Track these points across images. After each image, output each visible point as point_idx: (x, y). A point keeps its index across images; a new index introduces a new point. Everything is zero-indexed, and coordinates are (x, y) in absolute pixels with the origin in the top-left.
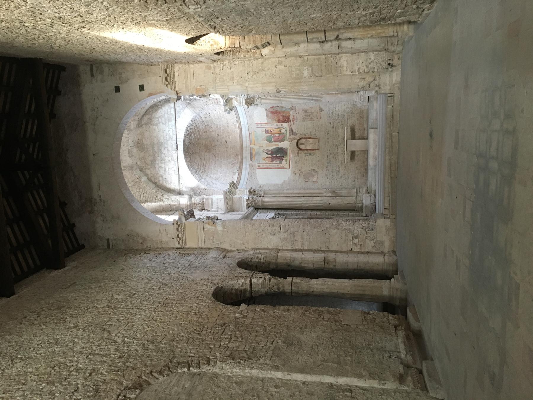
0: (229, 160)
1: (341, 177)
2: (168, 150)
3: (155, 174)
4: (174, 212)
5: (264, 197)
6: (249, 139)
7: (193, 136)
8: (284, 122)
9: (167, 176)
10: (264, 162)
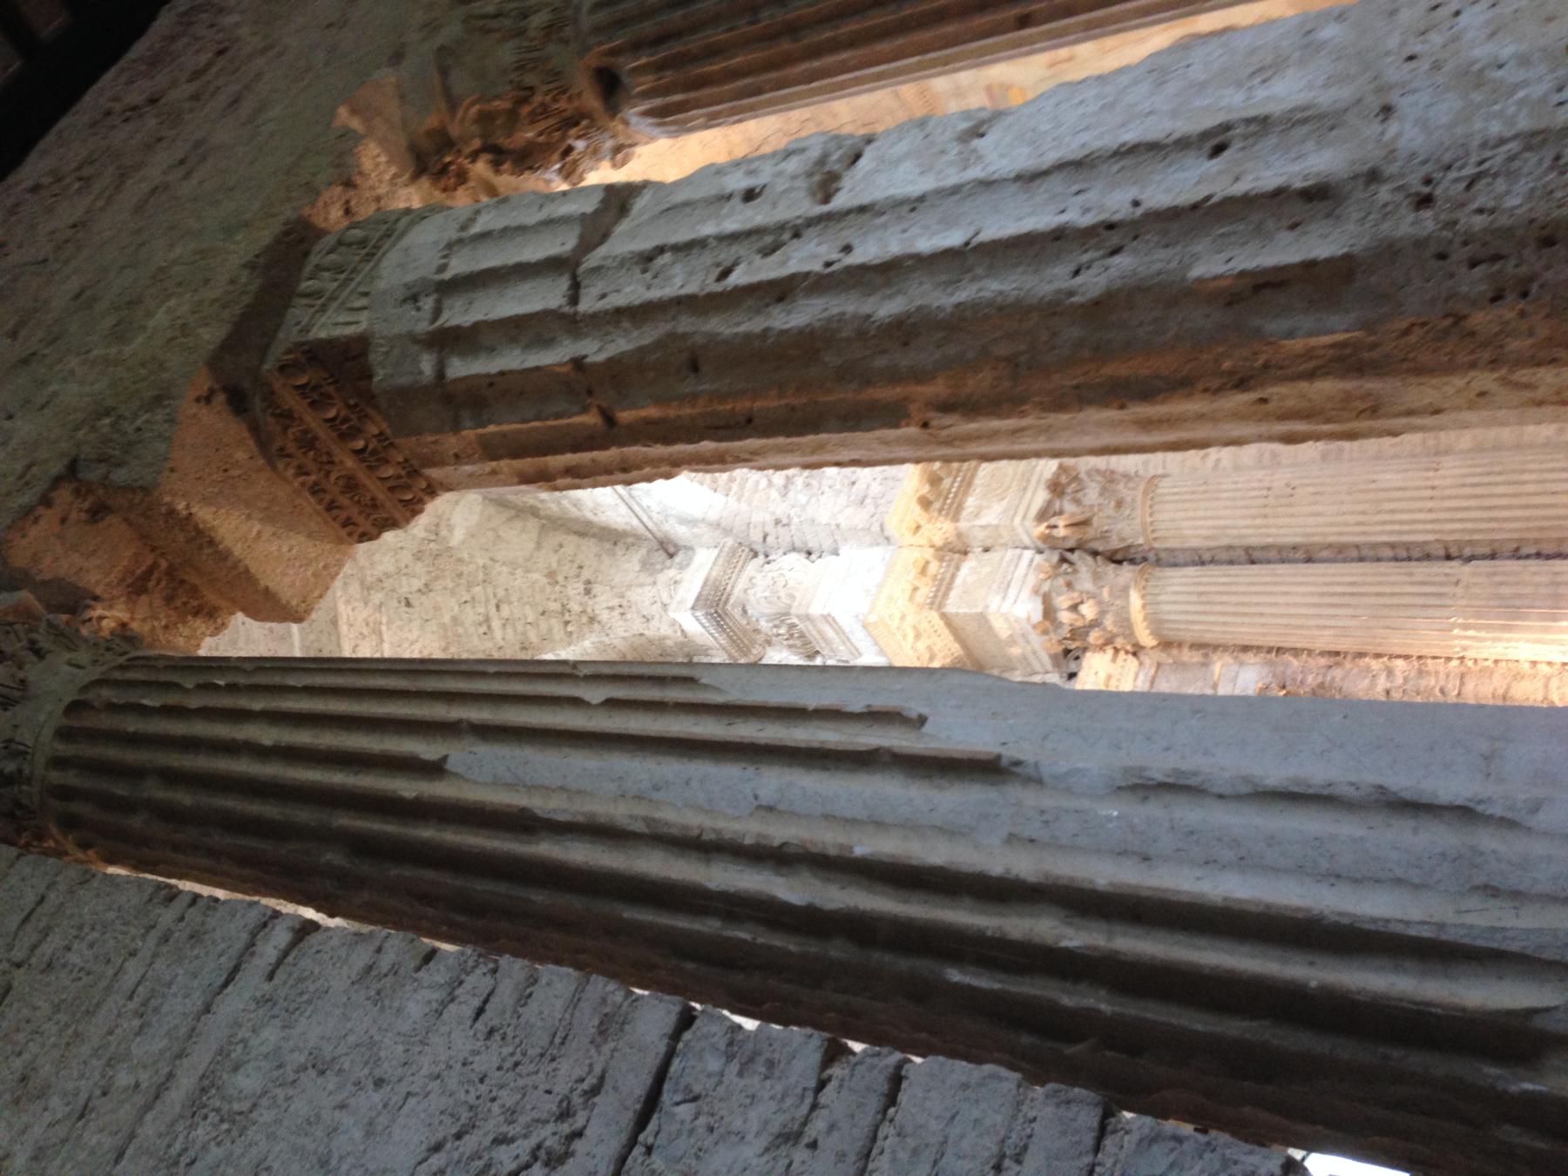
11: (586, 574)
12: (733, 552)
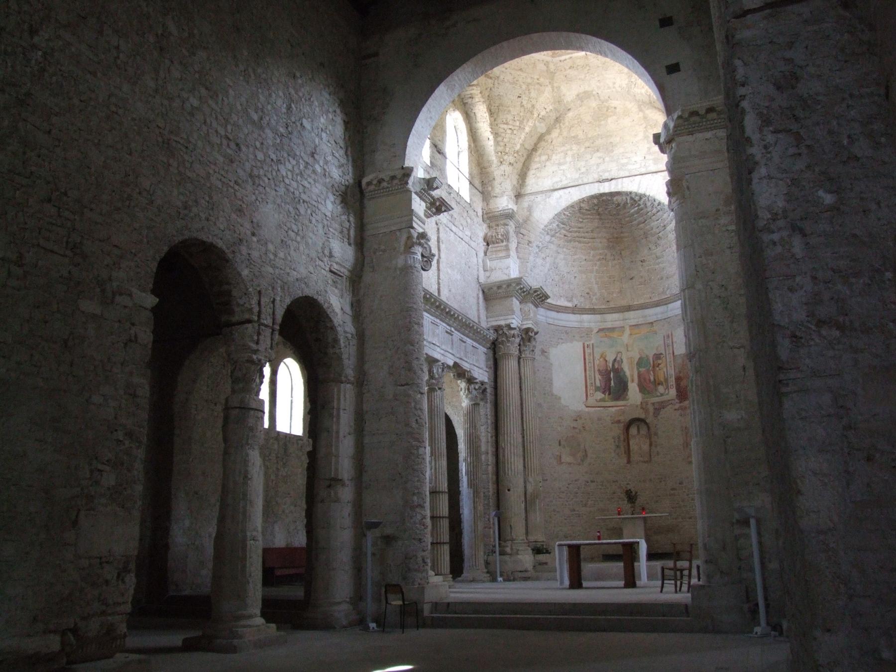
0: (596, 287)
1: (574, 510)
2: (598, 165)
3: (551, 147)
4: (480, 189)
5: (519, 358)
6: (640, 323)
7: (633, 211)
8: (679, 389)
9: (550, 168)
10: (597, 356)
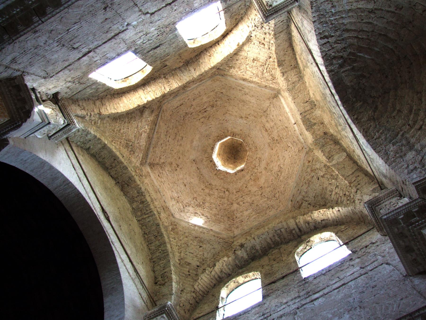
7: (366, 56)
11: (359, 186)
12: (392, 192)
